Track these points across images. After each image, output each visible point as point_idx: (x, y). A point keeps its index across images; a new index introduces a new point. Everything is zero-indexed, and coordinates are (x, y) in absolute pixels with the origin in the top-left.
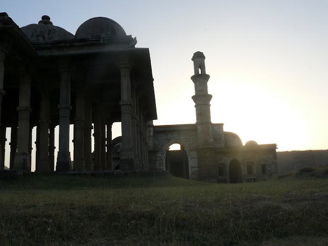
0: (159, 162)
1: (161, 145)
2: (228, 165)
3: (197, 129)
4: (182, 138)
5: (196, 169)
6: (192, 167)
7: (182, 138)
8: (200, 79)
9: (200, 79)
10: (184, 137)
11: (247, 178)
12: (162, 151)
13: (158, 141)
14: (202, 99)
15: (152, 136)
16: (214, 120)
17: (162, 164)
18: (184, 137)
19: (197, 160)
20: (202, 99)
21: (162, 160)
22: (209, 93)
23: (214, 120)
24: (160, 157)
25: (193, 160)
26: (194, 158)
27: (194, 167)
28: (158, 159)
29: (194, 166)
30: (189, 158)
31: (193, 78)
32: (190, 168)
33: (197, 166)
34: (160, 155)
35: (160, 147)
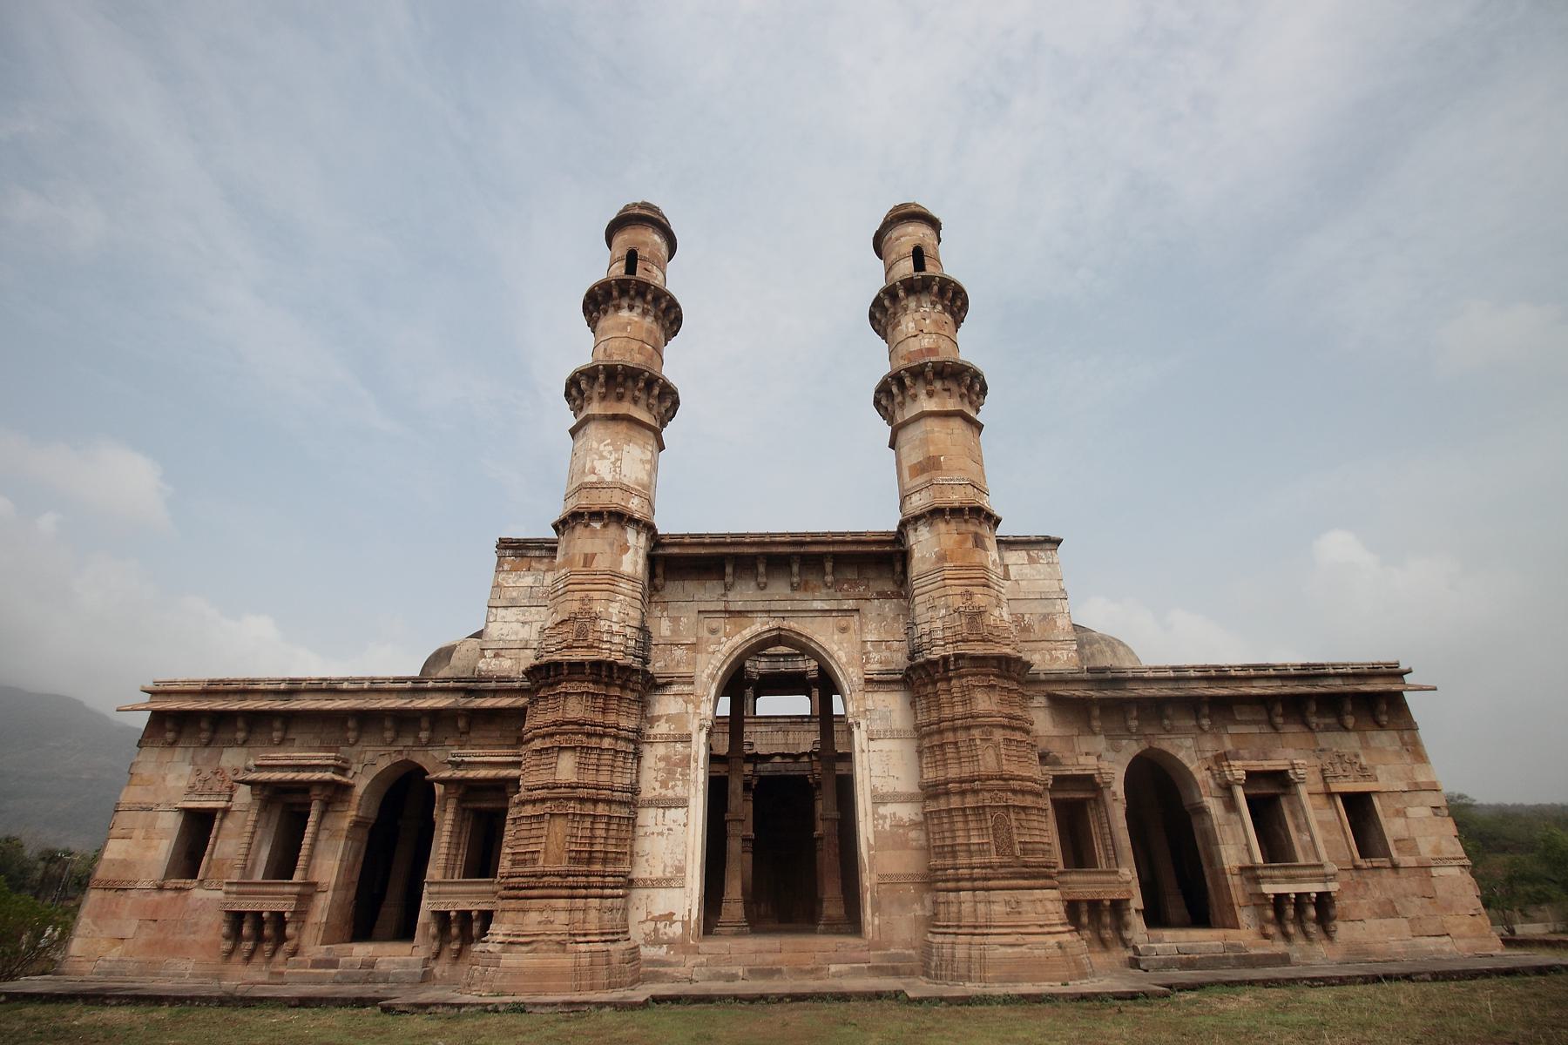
0: (661, 750)
1: (693, 647)
2: (1119, 787)
6: (879, 799)
7: (818, 605)
15: (631, 579)
17: (686, 762)
18: (833, 605)
21: (686, 739)
24: (669, 718)
26: (892, 735)
27: (896, 798)
28: (661, 728)
29: (888, 786)
33: (915, 789)
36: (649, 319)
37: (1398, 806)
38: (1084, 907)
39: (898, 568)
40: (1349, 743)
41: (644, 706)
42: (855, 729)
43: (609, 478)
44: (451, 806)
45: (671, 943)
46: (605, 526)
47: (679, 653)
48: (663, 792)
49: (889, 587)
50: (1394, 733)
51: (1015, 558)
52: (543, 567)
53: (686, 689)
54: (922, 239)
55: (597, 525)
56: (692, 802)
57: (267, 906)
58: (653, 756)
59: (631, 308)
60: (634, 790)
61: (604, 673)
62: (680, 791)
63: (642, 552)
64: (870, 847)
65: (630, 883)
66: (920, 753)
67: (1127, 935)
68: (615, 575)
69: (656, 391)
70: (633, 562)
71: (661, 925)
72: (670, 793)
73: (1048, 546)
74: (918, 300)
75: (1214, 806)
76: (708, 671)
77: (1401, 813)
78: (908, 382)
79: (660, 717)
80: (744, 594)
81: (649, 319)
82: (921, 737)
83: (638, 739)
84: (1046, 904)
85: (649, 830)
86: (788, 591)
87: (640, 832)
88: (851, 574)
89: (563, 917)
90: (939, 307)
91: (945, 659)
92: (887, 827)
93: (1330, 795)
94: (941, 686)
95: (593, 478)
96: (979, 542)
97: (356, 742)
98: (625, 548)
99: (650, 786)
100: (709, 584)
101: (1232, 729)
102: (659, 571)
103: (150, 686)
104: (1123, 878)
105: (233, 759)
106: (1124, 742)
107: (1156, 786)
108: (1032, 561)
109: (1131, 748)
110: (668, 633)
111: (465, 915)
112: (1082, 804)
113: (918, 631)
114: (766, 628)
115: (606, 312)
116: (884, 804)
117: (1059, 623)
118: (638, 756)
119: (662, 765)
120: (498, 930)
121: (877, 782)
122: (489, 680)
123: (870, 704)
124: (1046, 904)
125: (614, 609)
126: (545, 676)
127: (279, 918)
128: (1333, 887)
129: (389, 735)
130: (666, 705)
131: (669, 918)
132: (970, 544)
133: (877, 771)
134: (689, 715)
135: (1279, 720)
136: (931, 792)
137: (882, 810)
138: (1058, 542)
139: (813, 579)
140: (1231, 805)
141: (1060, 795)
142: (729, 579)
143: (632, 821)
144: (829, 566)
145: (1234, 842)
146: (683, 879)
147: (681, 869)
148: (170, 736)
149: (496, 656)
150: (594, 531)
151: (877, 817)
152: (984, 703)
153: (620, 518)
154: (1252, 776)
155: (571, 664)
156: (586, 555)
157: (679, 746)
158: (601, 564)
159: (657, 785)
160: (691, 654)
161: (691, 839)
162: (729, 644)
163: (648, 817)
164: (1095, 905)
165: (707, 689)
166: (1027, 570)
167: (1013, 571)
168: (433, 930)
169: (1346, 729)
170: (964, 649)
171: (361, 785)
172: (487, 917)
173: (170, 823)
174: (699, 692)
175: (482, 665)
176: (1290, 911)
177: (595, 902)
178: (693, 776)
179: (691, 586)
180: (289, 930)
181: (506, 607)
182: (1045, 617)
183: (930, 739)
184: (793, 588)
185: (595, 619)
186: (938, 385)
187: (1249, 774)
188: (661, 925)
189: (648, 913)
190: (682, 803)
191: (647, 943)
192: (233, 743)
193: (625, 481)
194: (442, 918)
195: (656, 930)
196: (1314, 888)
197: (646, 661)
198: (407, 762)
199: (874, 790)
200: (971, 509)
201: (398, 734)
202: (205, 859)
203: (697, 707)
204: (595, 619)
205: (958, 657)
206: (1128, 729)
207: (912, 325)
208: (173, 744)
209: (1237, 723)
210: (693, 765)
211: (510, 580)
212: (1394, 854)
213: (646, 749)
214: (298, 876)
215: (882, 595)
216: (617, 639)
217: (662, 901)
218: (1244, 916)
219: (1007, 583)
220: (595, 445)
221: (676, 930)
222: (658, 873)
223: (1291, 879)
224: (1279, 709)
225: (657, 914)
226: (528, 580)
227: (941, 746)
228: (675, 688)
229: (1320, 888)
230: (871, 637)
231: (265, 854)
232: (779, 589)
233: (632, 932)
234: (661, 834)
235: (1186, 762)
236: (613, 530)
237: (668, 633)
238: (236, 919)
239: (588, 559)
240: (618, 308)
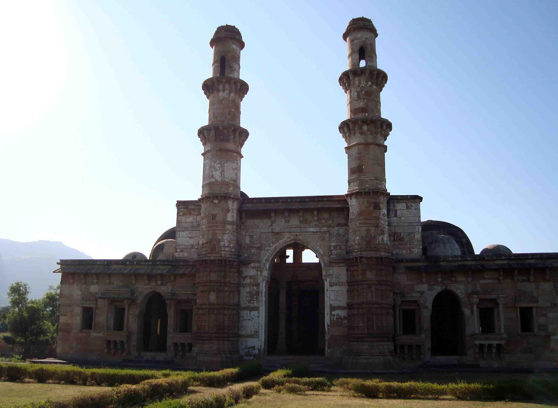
0: (248, 289)
2: (430, 305)
3: (348, 209)
4: (311, 229)
5: (342, 313)
6: (333, 308)
7: (311, 229)
8: (364, 80)
9: (364, 80)
10: (318, 229)
11: (477, 342)
12: (259, 262)
13: (251, 237)
14: (366, 130)
15: (231, 223)
16: (395, 186)
17: (258, 293)
18: (318, 229)
19: (345, 289)
20: (366, 130)
21: (258, 285)
22: (384, 115)
23: (395, 186)
24: (251, 277)
25: (337, 288)
27: (339, 308)
28: (248, 281)
29: (336, 304)
30: (327, 285)
31: (346, 80)
32: (327, 310)
34: (252, 272)
35: (253, 251)
36: (232, 95)
37: (544, 313)
38: (406, 348)
39: (346, 213)
40: (530, 287)
41: (240, 272)
42: (325, 281)
43: (219, 180)
44: (173, 308)
45: (255, 355)
46: (219, 202)
47: (253, 251)
48: (249, 305)
49: (342, 221)
50: (552, 284)
51: (400, 206)
52: (196, 214)
53: (257, 265)
54: (364, 42)
55: (216, 201)
56: (261, 309)
57: (118, 339)
58: (245, 292)
59: (224, 91)
60: (238, 305)
61: (223, 263)
62: (255, 304)
63: (235, 211)
64: (328, 326)
65: (240, 336)
66: (348, 291)
67: (422, 357)
68: (225, 222)
70: (231, 217)
71: (251, 350)
72: (252, 305)
73: (417, 200)
74: (360, 81)
75: (467, 312)
76: (265, 258)
77: (545, 315)
78: (351, 127)
79: (246, 277)
80: (280, 224)
82: (349, 286)
83: (239, 286)
84: (388, 346)
85: (245, 318)
86: (298, 223)
87: (241, 319)
88: (325, 215)
89: (215, 347)
90: (370, 83)
91: (357, 258)
92: (335, 319)
93: (517, 307)
94: (355, 268)
95: (213, 180)
96: (377, 207)
97: (135, 284)
98: (228, 211)
99: (244, 302)
100: (265, 221)
101: (482, 282)
102: (243, 216)
103: (59, 262)
104: (424, 338)
105: (94, 289)
106: (435, 287)
107: (447, 304)
108: (408, 207)
109: (438, 289)
110: (249, 242)
111: (183, 344)
112: (414, 311)
113: (349, 244)
114: (289, 240)
115: (212, 93)
116: (335, 310)
117: (416, 236)
118: (239, 292)
119: (248, 295)
120: (195, 349)
121: (332, 302)
122: (180, 261)
123: (331, 272)
124: (388, 346)
125: (226, 237)
126: (203, 264)
127: (122, 342)
128: (503, 342)
129: (146, 282)
130: (250, 271)
131: (253, 348)
132: (372, 208)
133: (332, 297)
134: (259, 275)
135: (501, 278)
136: (350, 306)
137: (333, 313)
138: (420, 199)
139: (309, 217)
140: (472, 312)
141: (404, 308)
142: (273, 219)
143: (238, 314)
144: (315, 213)
145: (473, 325)
146: (258, 335)
147: (257, 332)
148: (71, 281)
149: (181, 251)
150: (215, 204)
151: (331, 315)
152: (370, 275)
153: (226, 197)
154: (481, 300)
155: (210, 260)
156: (213, 215)
157: (255, 288)
158: (219, 218)
159: (247, 302)
160: (258, 251)
161: (261, 321)
162: (274, 247)
163: (244, 313)
164: (410, 347)
165: (265, 265)
166: (405, 212)
167: (399, 213)
168: (172, 349)
169: (530, 282)
170: (364, 254)
171: (140, 299)
172: (191, 346)
173: (78, 310)
174: (262, 267)
175: (176, 255)
176: (486, 350)
177: (226, 342)
178: (260, 299)
179: (257, 221)
180: (126, 346)
181: (183, 231)
182: (410, 233)
183: (352, 285)
184: (301, 222)
185: (219, 241)
186: (365, 128)
187: (481, 300)
188: (251, 350)
189: (246, 346)
190: (257, 309)
191: (246, 355)
192: (93, 284)
193: (226, 180)
194: (176, 345)
195: (249, 351)
196: (495, 343)
197: (239, 256)
198: (153, 291)
199: (331, 305)
200: (373, 192)
201: (149, 281)
202: (93, 323)
203: (262, 273)
204: (219, 241)
205: (361, 258)
206: (437, 282)
207: (356, 94)
208: (73, 283)
209: (484, 279)
210: (260, 295)
211: (184, 219)
212: (536, 330)
213: (242, 289)
214: (125, 329)
215: (339, 225)
216: (227, 249)
217: (252, 342)
218: (470, 352)
219: (395, 219)
220: (213, 164)
221: (256, 351)
222: (249, 333)
223: (487, 339)
224: (502, 273)
225: (249, 346)
226: (190, 219)
227: (353, 291)
228: (252, 265)
229: (497, 342)
230: (333, 244)
231: (112, 322)
232: (295, 221)
233: (240, 352)
234: (250, 320)
235: (459, 294)
236: (223, 203)
237: (249, 242)
238: (109, 342)
239: (214, 217)
240: (218, 91)
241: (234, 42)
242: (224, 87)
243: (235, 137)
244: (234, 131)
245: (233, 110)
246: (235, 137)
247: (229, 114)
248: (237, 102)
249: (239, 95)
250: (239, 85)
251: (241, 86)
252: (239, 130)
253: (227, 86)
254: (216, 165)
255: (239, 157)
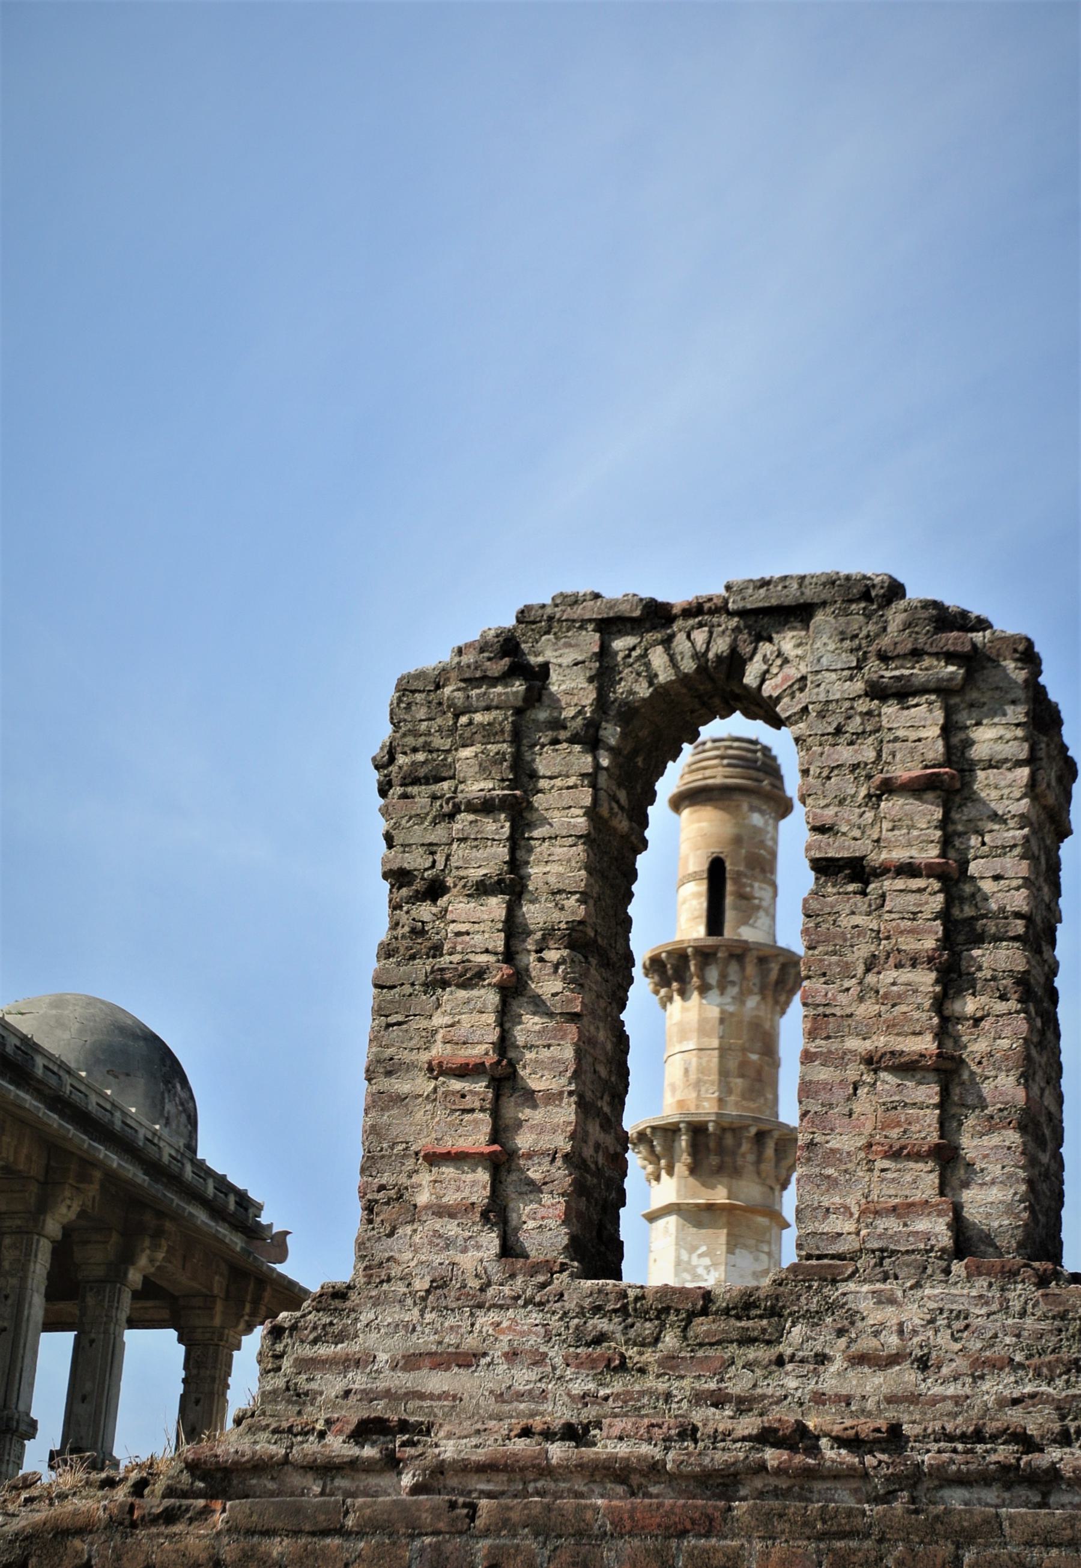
36: (752, 1002)
69: (770, 1152)
81: (752, 1002)
220: (685, 1256)
241: (756, 802)
242: (723, 976)
243: (759, 1160)
244: (760, 1137)
245: (754, 1057)
246: (759, 1160)
247: (742, 1076)
248: (767, 1026)
249: (776, 1002)
250: (775, 968)
251: (784, 968)
252: (776, 1134)
253: (733, 969)
254: (695, 1260)
255: (775, 1230)
